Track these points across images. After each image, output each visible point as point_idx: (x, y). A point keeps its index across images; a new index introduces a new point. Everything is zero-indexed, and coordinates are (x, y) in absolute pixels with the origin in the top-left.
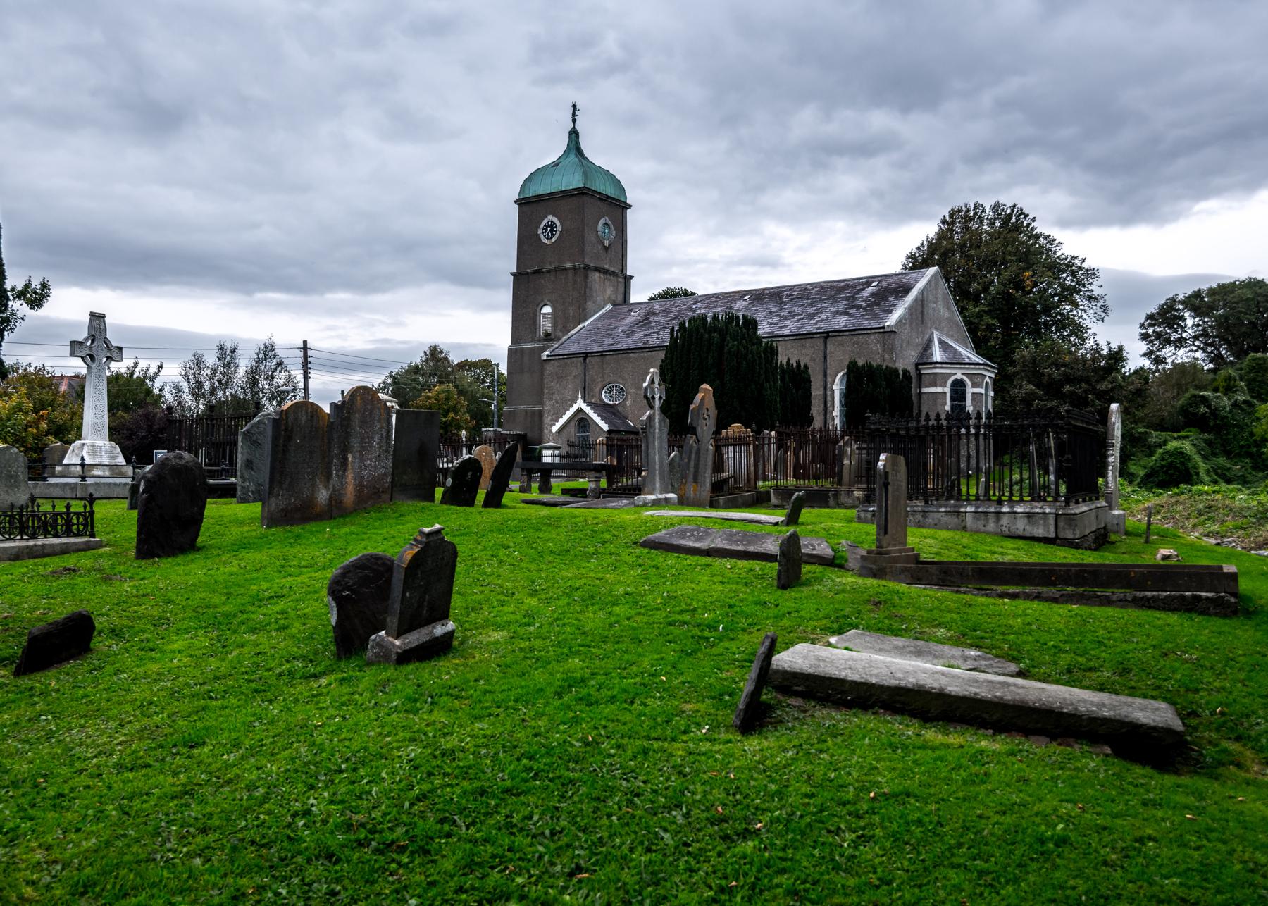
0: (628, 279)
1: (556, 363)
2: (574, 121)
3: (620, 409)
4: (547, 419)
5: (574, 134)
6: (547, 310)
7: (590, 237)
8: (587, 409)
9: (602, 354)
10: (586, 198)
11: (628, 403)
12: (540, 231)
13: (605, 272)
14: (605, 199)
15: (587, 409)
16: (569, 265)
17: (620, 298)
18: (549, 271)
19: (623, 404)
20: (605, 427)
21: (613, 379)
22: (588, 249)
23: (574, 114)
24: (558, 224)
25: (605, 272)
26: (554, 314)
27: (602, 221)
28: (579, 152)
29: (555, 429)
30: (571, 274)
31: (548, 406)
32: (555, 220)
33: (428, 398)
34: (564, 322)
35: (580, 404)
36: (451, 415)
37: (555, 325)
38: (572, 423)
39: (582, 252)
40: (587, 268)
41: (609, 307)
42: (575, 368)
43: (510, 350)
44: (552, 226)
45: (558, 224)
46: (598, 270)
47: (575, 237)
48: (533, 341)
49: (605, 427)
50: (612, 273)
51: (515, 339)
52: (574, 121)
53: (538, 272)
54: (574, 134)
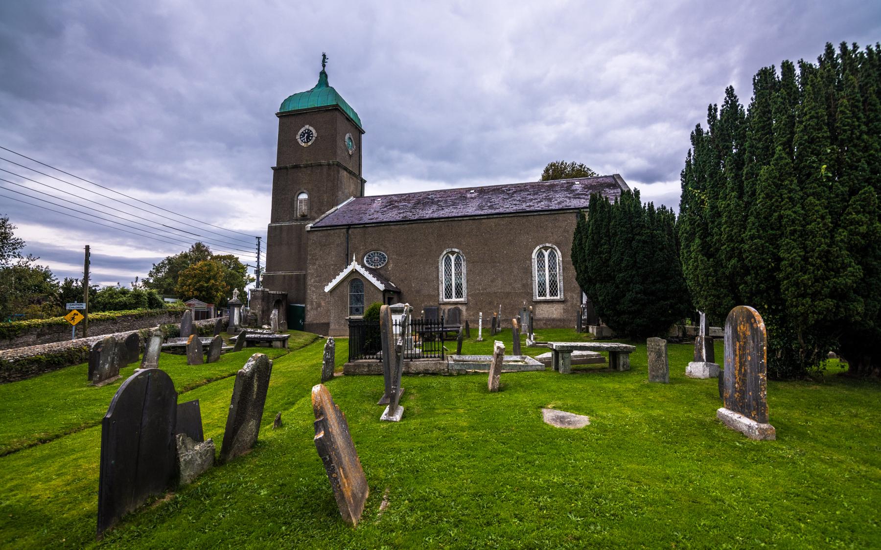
0: (363, 182)
1: (319, 234)
2: (324, 66)
3: (382, 272)
4: (311, 281)
5: (323, 75)
6: (304, 196)
7: (340, 143)
8: (362, 271)
9: (365, 226)
10: (337, 113)
11: (390, 267)
12: (298, 137)
13: (350, 172)
14: (349, 119)
15: (362, 271)
16: (323, 162)
17: (359, 195)
18: (306, 166)
19: (385, 268)
20: (381, 287)
21: (374, 247)
22: (339, 152)
23: (324, 61)
24: (314, 131)
25: (350, 172)
26: (310, 201)
27: (347, 136)
28: (327, 85)
29: (327, 289)
30: (325, 169)
31: (311, 269)
32: (311, 128)
33: (194, 269)
34: (318, 205)
35: (354, 265)
36: (212, 281)
37: (310, 208)
38: (345, 283)
39: (335, 154)
40: (339, 165)
41: (352, 199)
42: (339, 238)
43: (270, 227)
44: (309, 133)
45: (314, 131)
46: (346, 169)
47: (328, 141)
48: (291, 220)
49: (381, 287)
50: (354, 174)
51: (274, 220)
52: (324, 66)
53: (296, 167)
54: (323, 75)
